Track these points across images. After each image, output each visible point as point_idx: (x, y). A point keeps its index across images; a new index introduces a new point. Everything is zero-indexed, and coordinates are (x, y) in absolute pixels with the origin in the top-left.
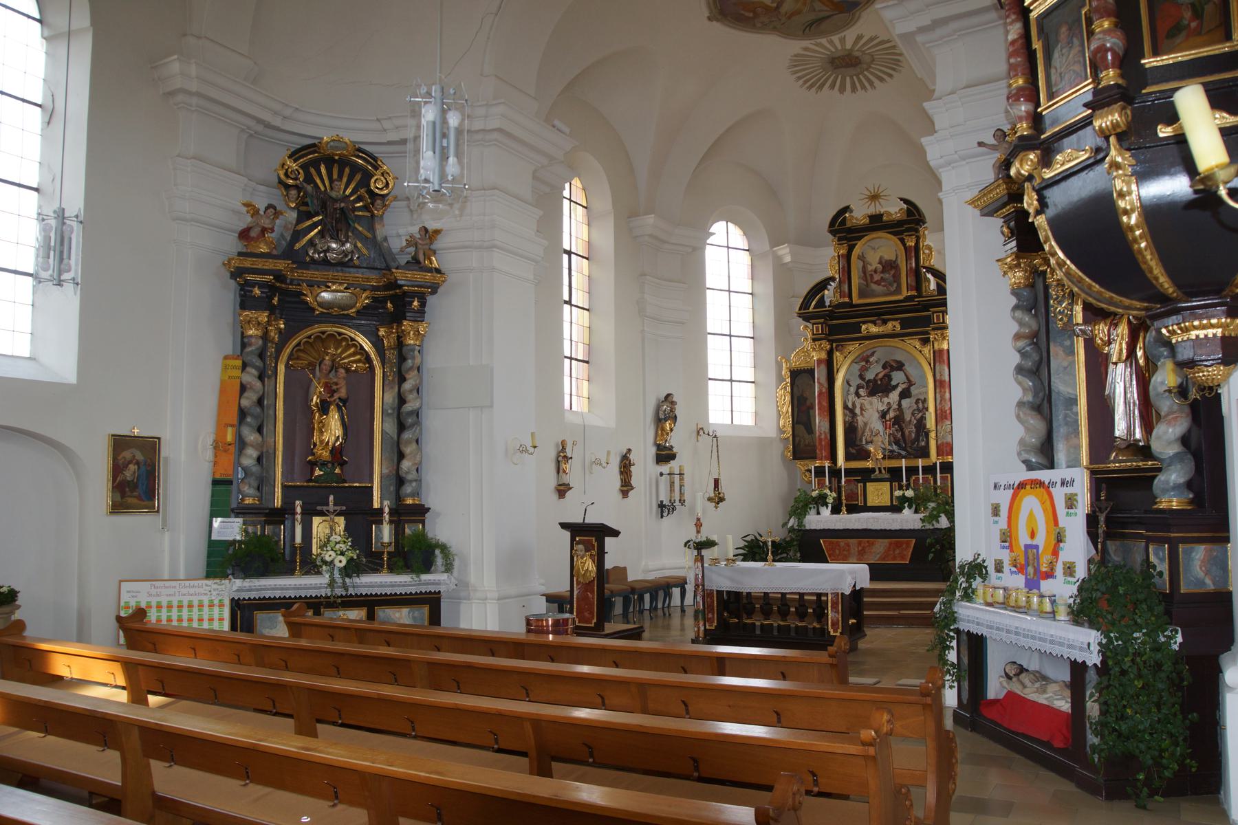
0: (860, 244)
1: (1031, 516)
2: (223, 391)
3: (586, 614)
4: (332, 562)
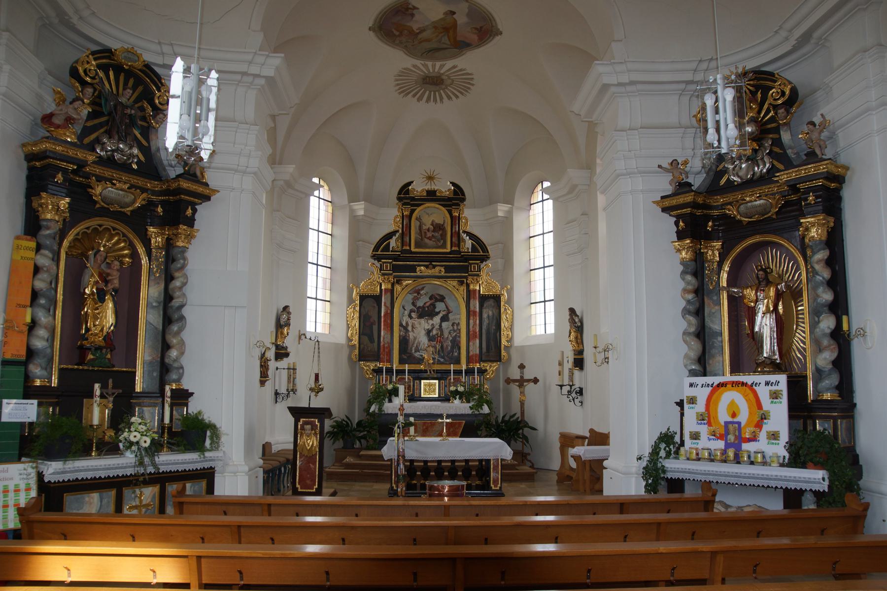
0: (419, 209)
1: (732, 403)
2: (13, 270)
3: (308, 482)
4: (137, 443)
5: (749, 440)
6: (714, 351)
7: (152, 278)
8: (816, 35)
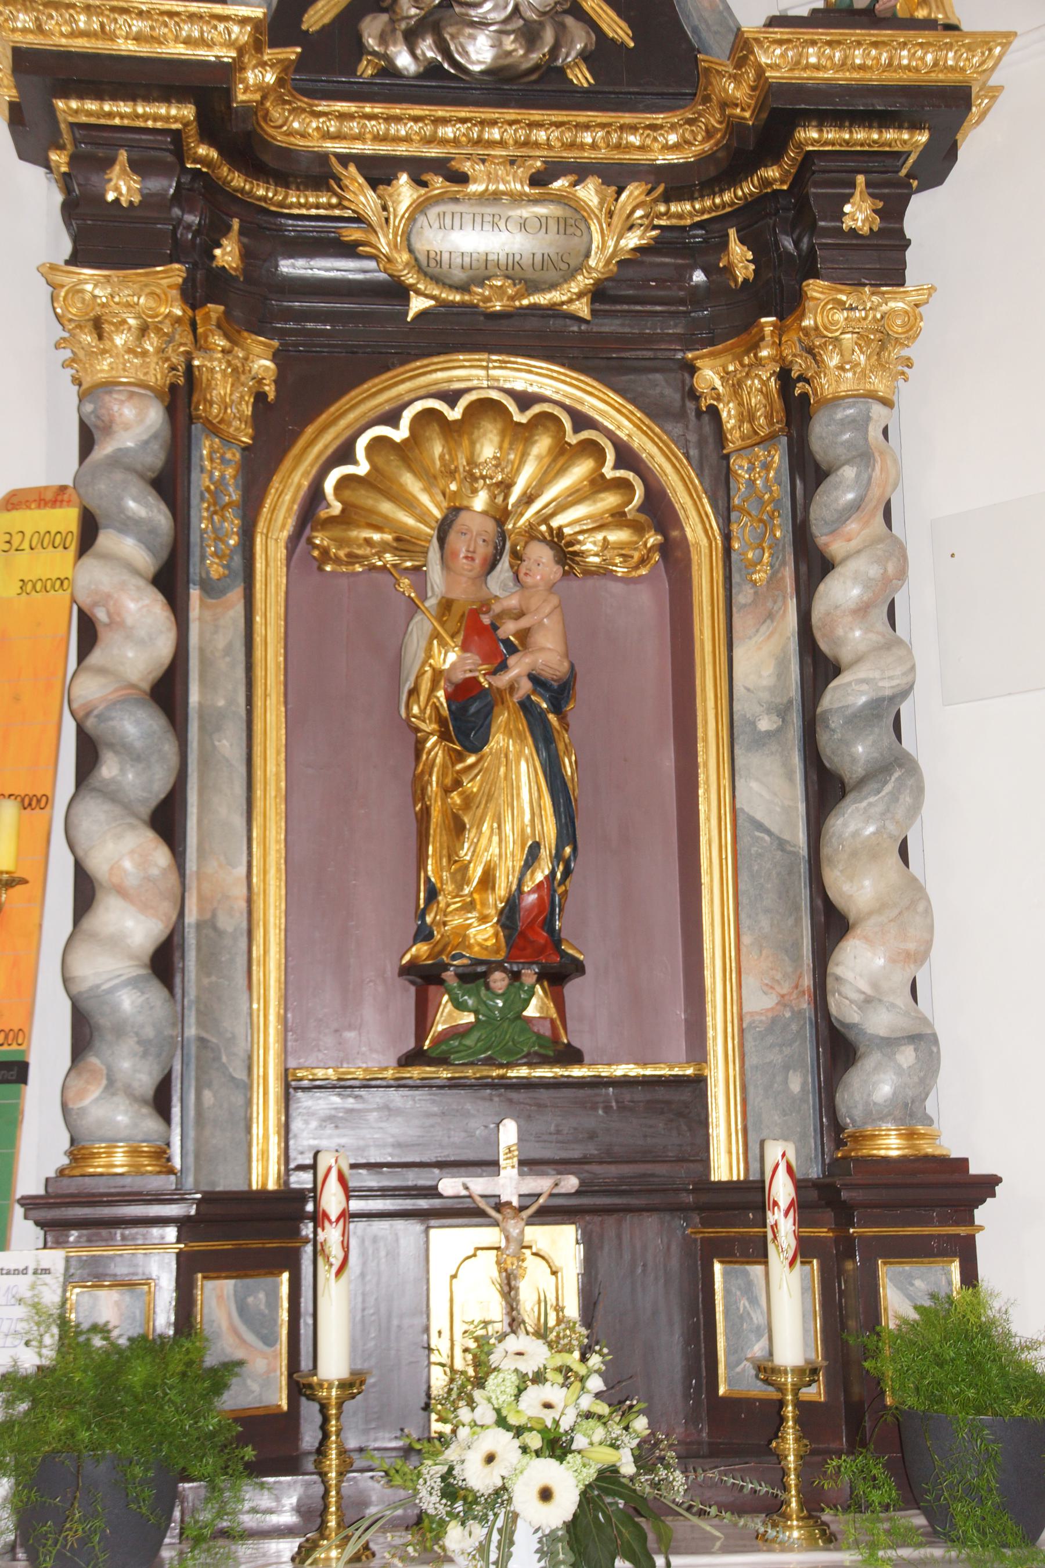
7: (743, 596)
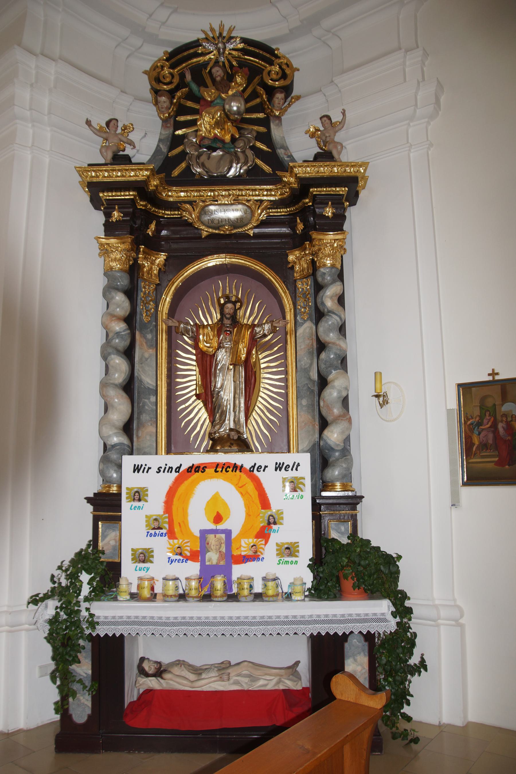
1: (216, 499)
5: (244, 559)
6: (145, 417)
8: (326, 23)
